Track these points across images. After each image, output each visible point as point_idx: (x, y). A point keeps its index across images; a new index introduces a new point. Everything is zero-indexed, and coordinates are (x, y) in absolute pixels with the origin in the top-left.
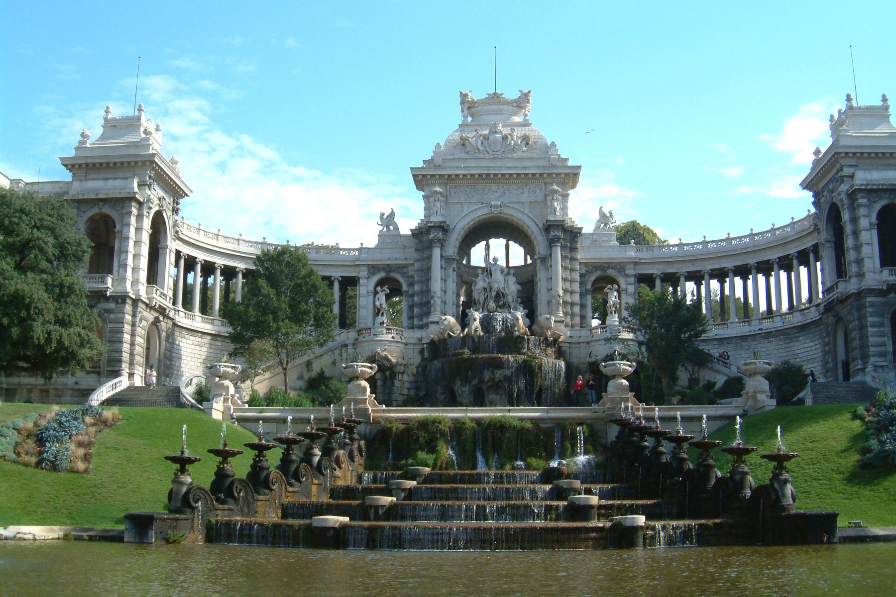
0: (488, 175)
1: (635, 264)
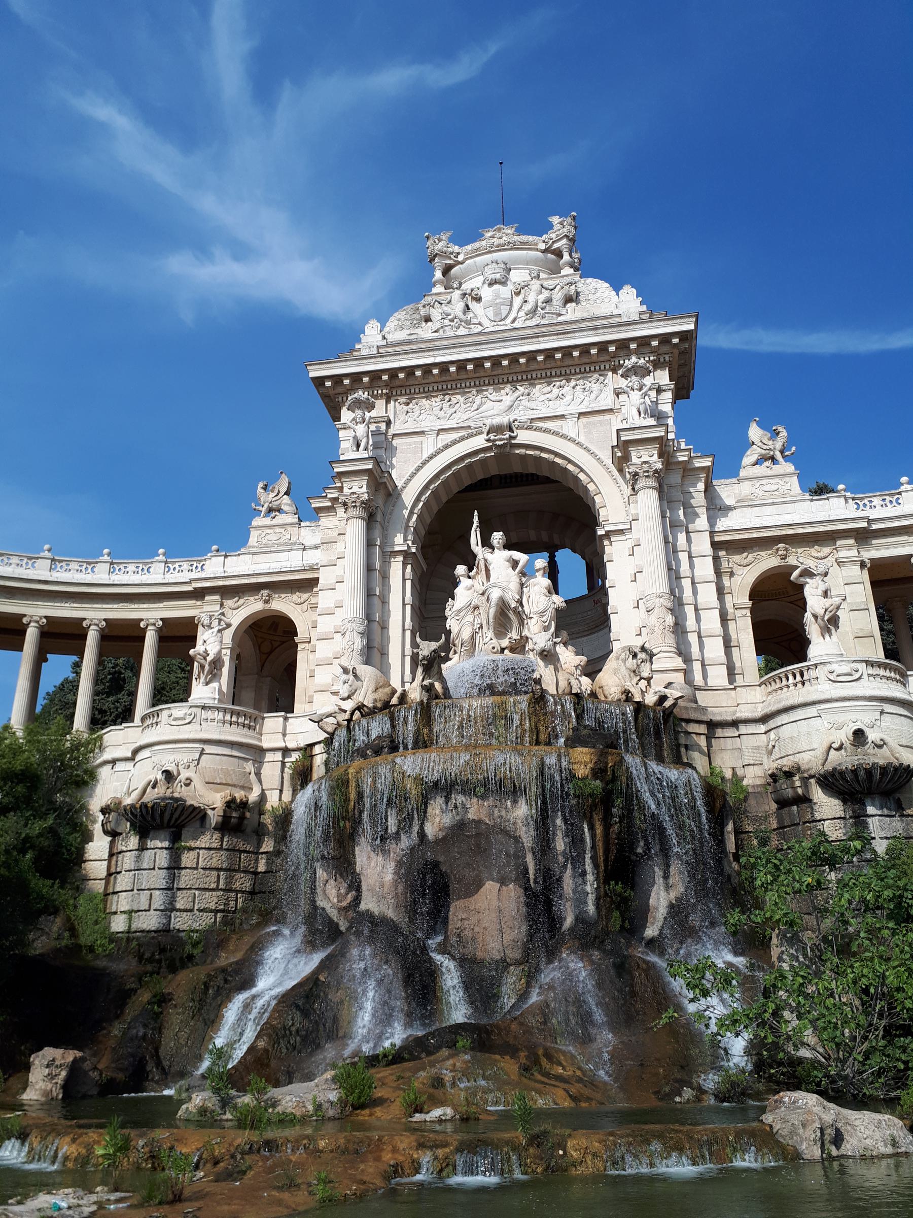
1: (863, 536)
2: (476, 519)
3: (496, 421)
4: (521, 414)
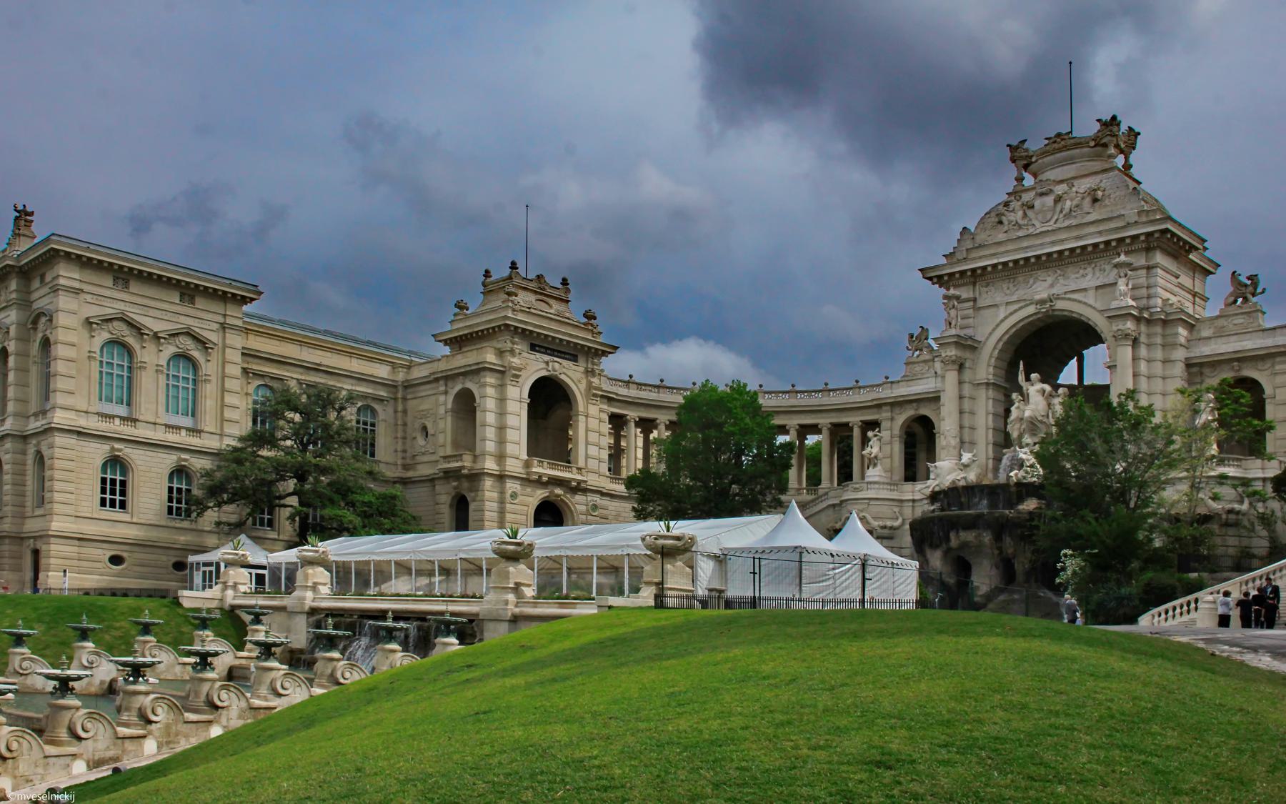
0: (1027, 259)
2: (1021, 366)
3: (1037, 297)
4: (1055, 291)
